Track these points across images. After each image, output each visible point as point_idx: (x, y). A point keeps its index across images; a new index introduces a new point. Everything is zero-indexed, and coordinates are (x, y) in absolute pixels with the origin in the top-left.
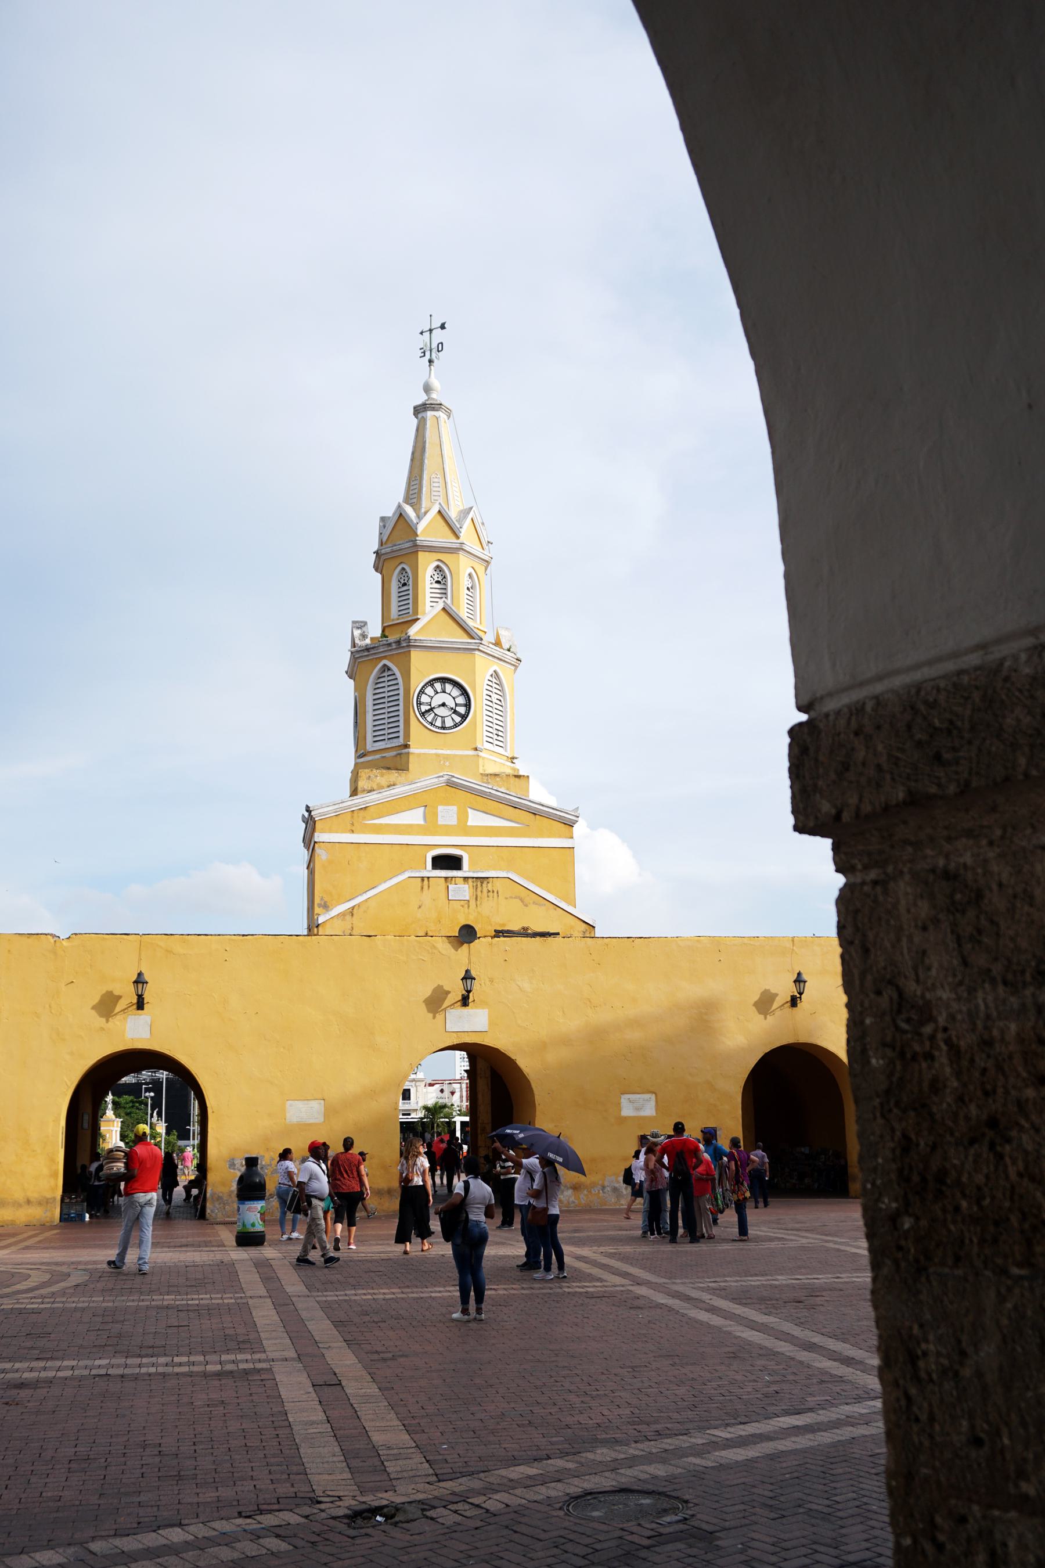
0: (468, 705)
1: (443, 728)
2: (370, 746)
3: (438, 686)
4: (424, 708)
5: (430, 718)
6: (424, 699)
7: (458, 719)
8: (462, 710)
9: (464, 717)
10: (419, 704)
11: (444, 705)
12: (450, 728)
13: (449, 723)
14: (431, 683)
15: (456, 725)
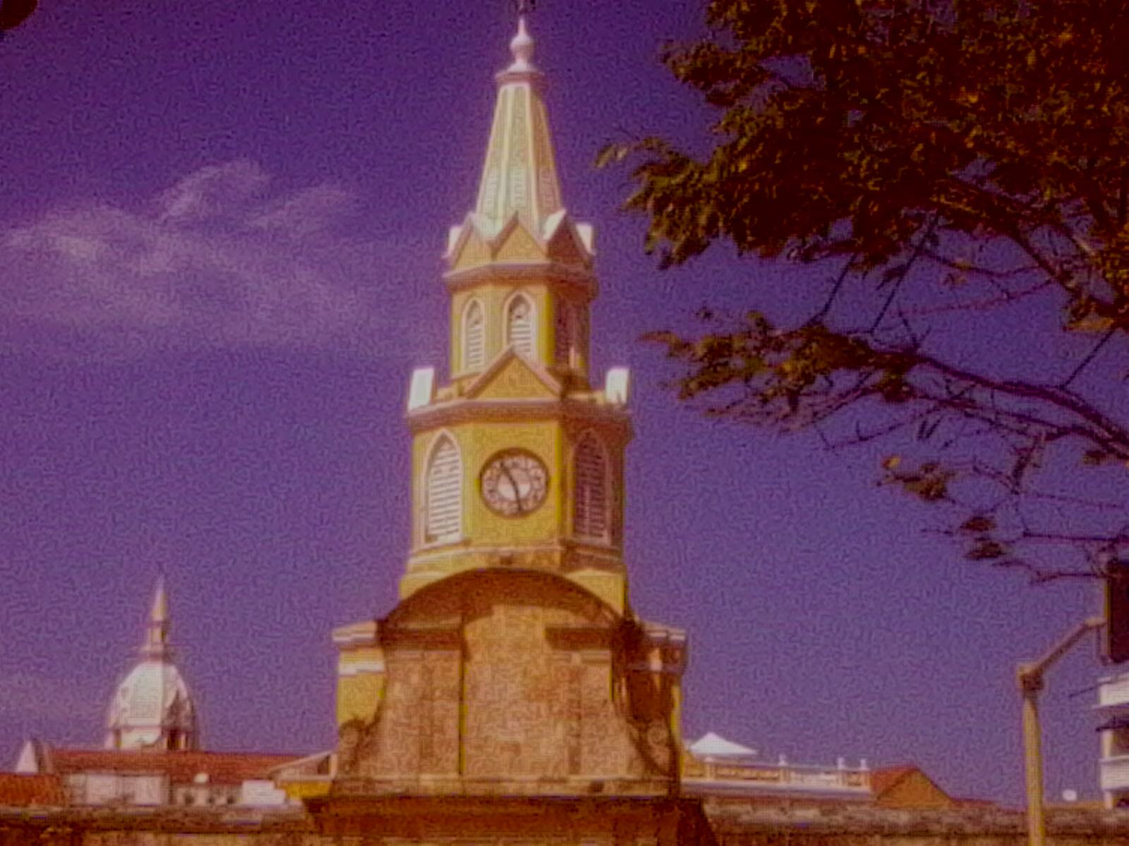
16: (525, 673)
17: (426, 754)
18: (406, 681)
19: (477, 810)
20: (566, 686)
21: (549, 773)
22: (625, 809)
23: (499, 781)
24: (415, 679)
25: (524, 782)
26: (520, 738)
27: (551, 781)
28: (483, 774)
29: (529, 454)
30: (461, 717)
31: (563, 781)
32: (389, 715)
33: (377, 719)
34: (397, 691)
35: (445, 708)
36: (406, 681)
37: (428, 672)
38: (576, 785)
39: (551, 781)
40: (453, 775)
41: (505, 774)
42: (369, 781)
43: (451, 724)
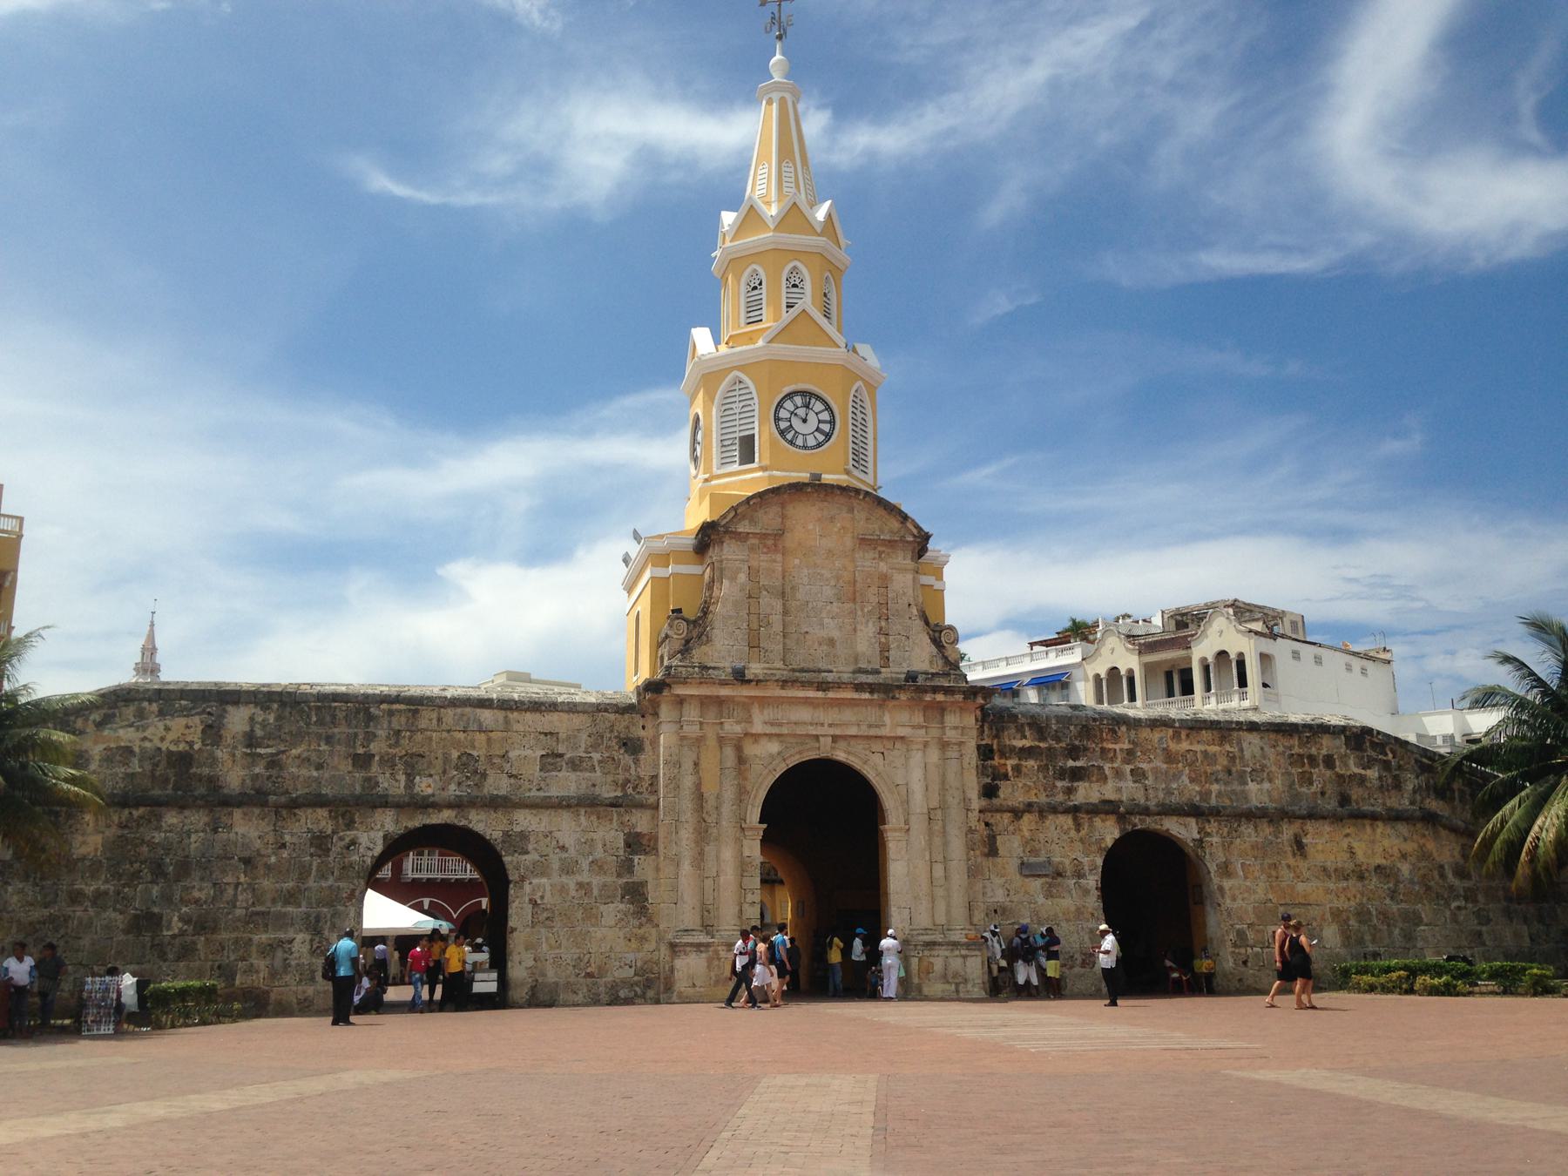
0: (832, 422)
1: (805, 447)
2: (716, 471)
3: (798, 400)
4: (783, 425)
5: (789, 437)
6: (783, 414)
7: (821, 438)
8: (826, 428)
9: (828, 436)
10: (777, 419)
11: (805, 421)
12: (813, 448)
13: (811, 442)
14: (790, 396)
15: (819, 445)
16: (838, 578)
17: (754, 644)
18: (733, 579)
19: (811, 694)
20: (874, 590)
21: (863, 665)
22: (940, 697)
23: (820, 671)
24: (742, 577)
25: (842, 671)
26: (835, 634)
27: (866, 672)
28: (803, 665)
29: (818, 398)
30: (785, 613)
31: (877, 672)
32: (718, 609)
33: (705, 612)
34: (725, 589)
35: (770, 604)
36: (733, 579)
37: (753, 573)
38: (894, 672)
39: (866, 672)
40: (779, 665)
41: (822, 665)
42: (704, 668)
43: (776, 619)
